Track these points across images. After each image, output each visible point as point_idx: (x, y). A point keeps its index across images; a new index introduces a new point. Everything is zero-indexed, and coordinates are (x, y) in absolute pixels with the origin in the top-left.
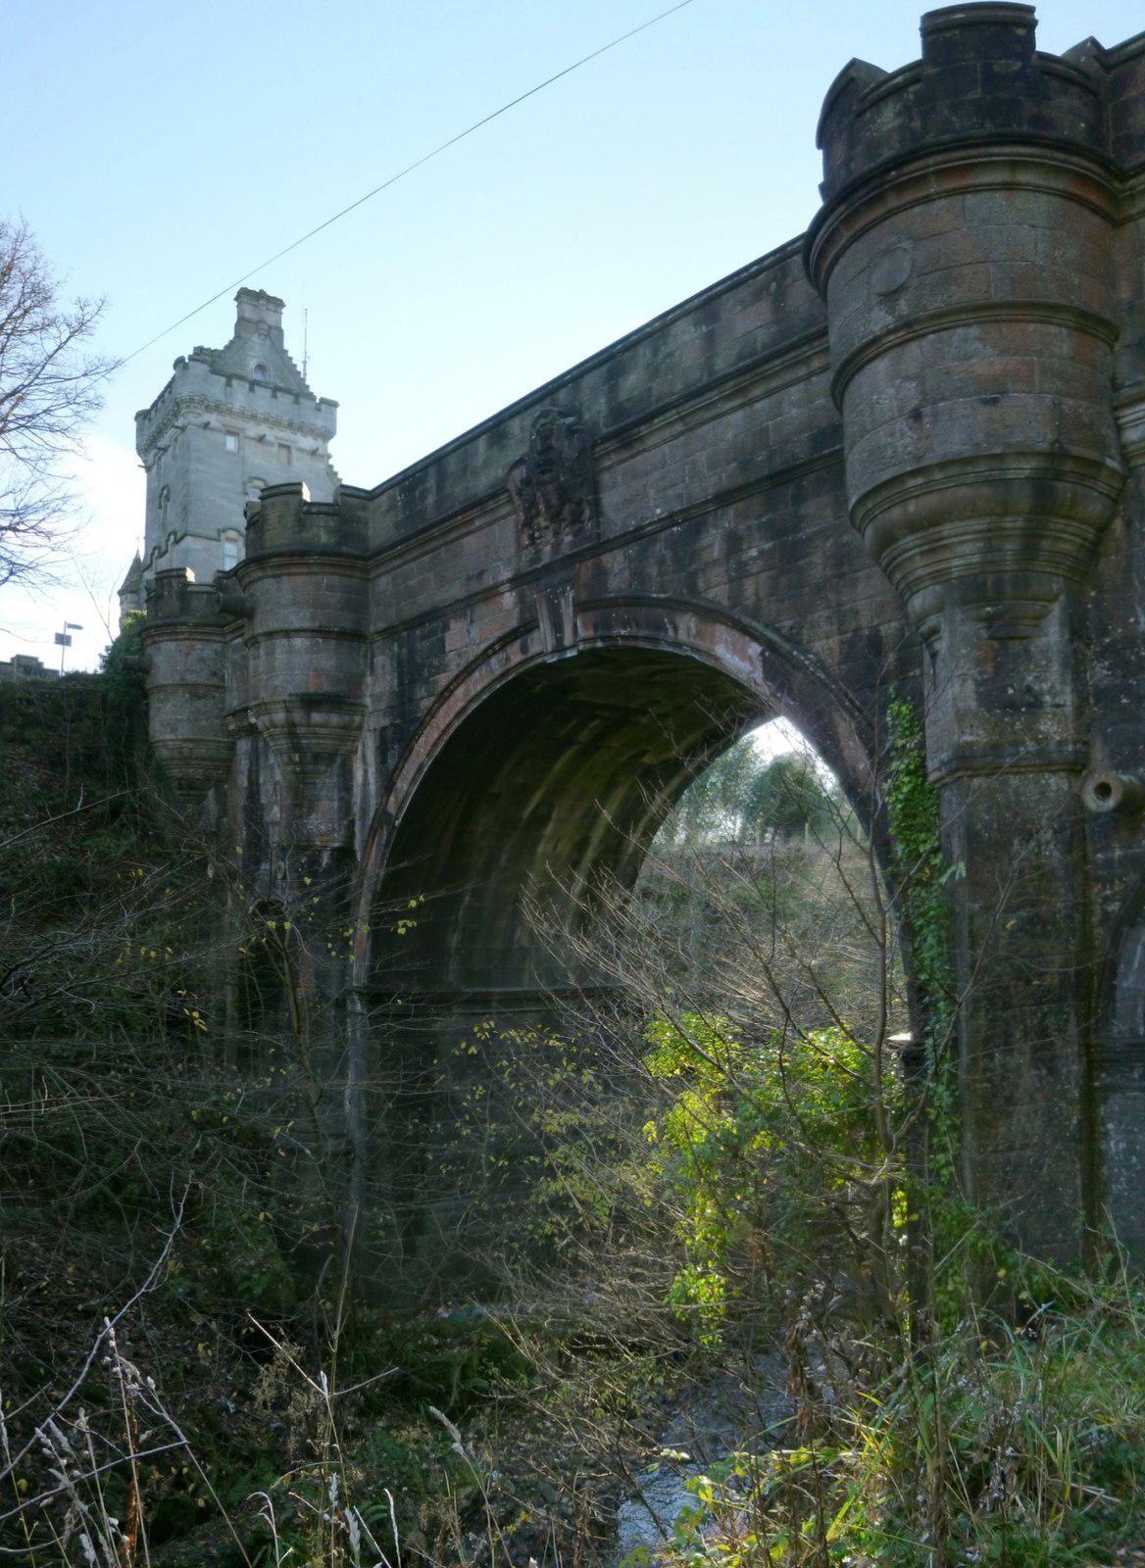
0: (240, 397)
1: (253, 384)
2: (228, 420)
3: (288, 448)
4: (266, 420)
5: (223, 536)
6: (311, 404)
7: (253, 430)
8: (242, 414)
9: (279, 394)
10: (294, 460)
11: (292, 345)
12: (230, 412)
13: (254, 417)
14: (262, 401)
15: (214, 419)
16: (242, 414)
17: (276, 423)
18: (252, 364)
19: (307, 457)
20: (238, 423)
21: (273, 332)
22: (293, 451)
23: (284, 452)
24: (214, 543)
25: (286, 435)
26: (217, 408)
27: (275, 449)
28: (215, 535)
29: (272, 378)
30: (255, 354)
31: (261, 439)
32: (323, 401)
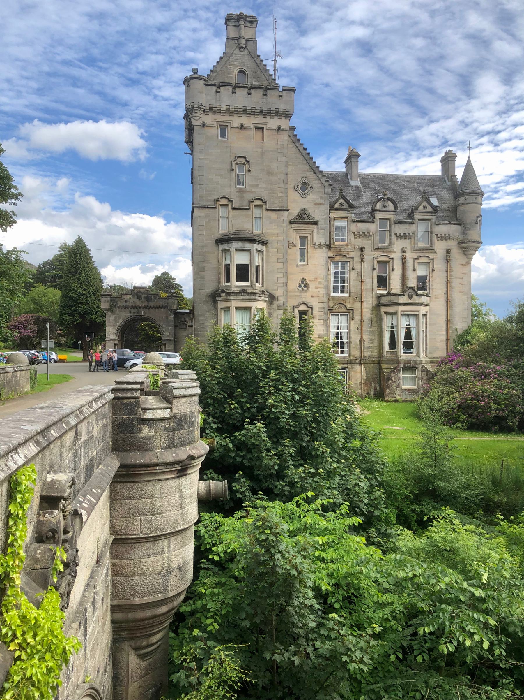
0: (227, 99)
1: (237, 86)
2: (219, 117)
3: (262, 128)
5: (218, 204)
6: (276, 93)
7: (236, 121)
8: (229, 112)
9: (253, 91)
10: (266, 137)
13: (237, 111)
14: (241, 99)
16: (229, 112)
19: (275, 133)
21: (250, 43)
22: (266, 132)
23: (259, 133)
24: (211, 210)
25: (260, 120)
26: (211, 110)
28: (211, 204)
29: (249, 81)
31: (242, 127)
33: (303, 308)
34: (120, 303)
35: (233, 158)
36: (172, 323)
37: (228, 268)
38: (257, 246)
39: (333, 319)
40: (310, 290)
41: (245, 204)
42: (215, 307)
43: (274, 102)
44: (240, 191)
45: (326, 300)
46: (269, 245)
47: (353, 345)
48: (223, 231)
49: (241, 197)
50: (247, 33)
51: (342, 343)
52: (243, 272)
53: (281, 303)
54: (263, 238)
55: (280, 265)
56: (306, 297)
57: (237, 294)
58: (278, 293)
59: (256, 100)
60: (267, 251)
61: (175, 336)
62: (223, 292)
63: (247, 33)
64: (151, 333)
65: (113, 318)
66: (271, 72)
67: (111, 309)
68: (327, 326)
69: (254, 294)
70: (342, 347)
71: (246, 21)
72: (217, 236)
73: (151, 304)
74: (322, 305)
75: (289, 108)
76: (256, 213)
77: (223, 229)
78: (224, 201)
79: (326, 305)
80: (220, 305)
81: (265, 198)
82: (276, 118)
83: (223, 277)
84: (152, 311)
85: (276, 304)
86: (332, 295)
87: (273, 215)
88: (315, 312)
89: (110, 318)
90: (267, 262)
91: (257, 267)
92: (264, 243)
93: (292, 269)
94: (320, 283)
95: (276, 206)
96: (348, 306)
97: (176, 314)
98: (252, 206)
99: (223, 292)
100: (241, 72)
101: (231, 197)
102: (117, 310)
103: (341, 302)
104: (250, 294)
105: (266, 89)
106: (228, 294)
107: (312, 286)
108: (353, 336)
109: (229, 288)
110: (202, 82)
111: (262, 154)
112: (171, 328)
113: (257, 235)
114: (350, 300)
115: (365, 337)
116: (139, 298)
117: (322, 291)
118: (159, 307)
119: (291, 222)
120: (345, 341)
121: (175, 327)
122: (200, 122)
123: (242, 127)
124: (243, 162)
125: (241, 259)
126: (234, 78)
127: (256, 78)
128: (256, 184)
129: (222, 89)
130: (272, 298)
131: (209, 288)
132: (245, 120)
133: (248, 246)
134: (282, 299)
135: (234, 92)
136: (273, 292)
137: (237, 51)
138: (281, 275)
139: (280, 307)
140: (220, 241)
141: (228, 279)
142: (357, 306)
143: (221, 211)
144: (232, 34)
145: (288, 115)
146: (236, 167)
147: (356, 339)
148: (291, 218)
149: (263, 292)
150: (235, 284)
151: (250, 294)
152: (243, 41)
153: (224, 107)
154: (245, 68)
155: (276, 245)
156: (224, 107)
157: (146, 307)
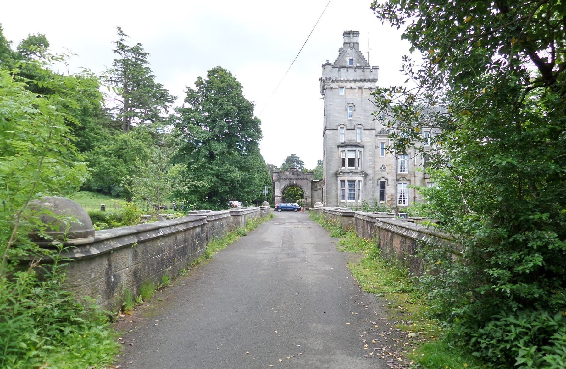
0: (344, 74)
1: (348, 68)
2: (340, 84)
4: (353, 80)
5: (339, 128)
6: (369, 70)
7: (348, 85)
8: (344, 81)
10: (363, 93)
11: (363, 49)
12: (340, 80)
14: (351, 74)
15: (334, 85)
16: (344, 81)
17: (357, 80)
18: (348, 60)
20: (344, 84)
21: (356, 45)
23: (360, 90)
25: (360, 84)
27: (357, 90)
28: (335, 128)
29: (355, 64)
30: (350, 54)
32: (374, 68)
33: (383, 180)
34: (283, 177)
35: (346, 104)
36: (310, 188)
37: (344, 159)
38: (358, 149)
39: (399, 185)
40: (387, 170)
41: (353, 127)
42: (337, 180)
43: (368, 75)
44: (350, 120)
45: (395, 176)
46: (365, 148)
47: (410, 200)
48: (341, 141)
49: (351, 123)
50: (354, 40)
51: (404, 198)
52: (351, 162)
53: (371, 178)
54: (362, 144)
55: (371, 158)
56: (384, 174)
57: (348, 173)
58: (370, 172)
59: (358, 74)
60: (364, 151)
61: (311, 195)
62: (341, 172)
63: (354, 40)
64: (291, 192)
65: (279, 184)
66: (366, 59)
67: (279, 180)
68: (396, 190)
69: (357, 173)
70: (404, 201)
71: (353, 34)
72: (338, 144)
73: (299, 177)
74: (393, 178)
75: (375, 77)
76: (358, 131)
77: (342, 140)
78: (342, 126)
79: (395, 178)
80: (339, 179)
81: (363, 124)
82: (369, 83)
83: (341, 164)
84: (299, 181)
85: (368, 178)
86: (399, 172)
87: (367, 132)
88: (389, 182)
89: (277, 184)
90: (364, 156)
91: (359, 159)
92: (362, 147)
93: (378, 160)
94: (392, 167)
95: (369, 128)
96: (408, 179)
97: (312, 182)
98: (356, 128)
99: (341, 172)
100: (351, 60)
101: (346, 124)
102: (281, 181)
103: (404, 177)
104: (355, 173)
105: (364, 68)
106: (344, 173)
107: (388, 169)
108: (410, 195)
109: (344, 170)
110: (331, 67)
111: (362, 101)
112: (309, 190)
113: (359, 143)
114: (409, 175)
115: (417, 196)
116: (293, 174)
117: (394, 171)
118: (303, 179)
119: (377, 135)
120: (405, 197)
121: (312, 189)
122: (330, 87)
123: (351, 88)
124: (351, 105)
125: (351, 155)
126: (347, 63)
127: (359, 63)
128: (359, 116)
129: (341, 69)
130: (366, 175)
131: (333, 171)
132: (353, 85)
133: (354, 149)
134: (372, 176)
135: (347, 71)
136: (367, 172)
137: (349, 49)
138: (371, 163)
139: (370, 180)
140: (339, 147)
141: (344, 166)
142: (412, 179)
143: (341, 131)
144: (346, 41)
145: (375, 81)
146: (348, 109)
147: (412, 196)
148: (377, 133)
149: (362, 172)
150: (347, 168)
151: (355, 173)
152: (352, 45)
153: (342, 79)
154: (352, 58)
155: (368, 148)
156: (342, 79)
157: (296, 179)
